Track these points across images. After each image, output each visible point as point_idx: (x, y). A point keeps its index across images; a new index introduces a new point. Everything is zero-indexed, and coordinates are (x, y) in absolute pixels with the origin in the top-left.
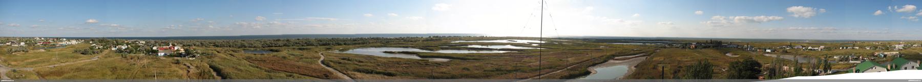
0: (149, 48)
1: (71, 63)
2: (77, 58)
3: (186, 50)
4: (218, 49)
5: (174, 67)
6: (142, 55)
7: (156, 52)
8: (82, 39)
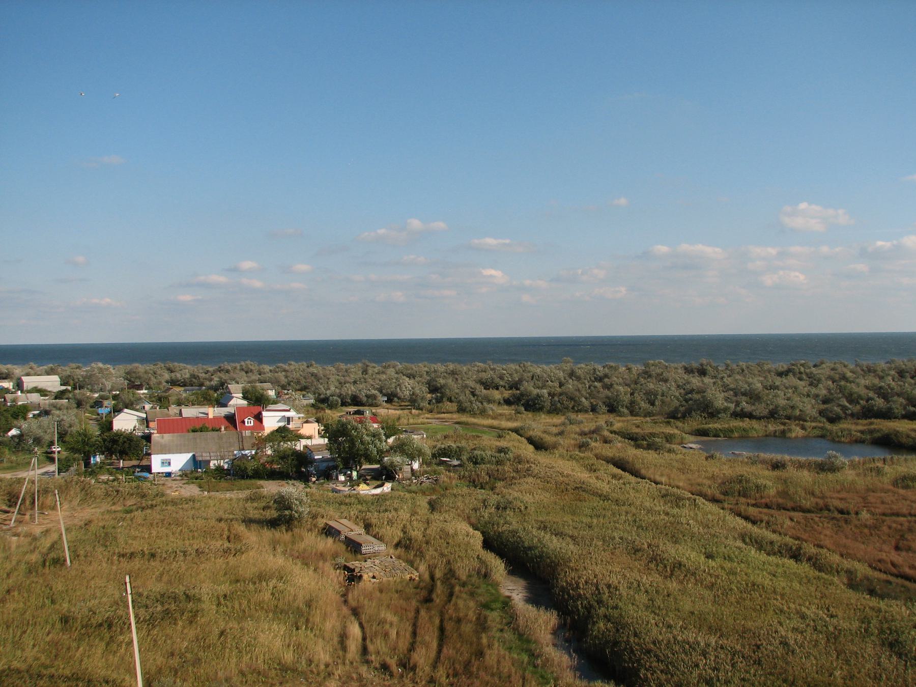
3: (334, 433)
5: (261, 551)
6: (35, 473)
7: (132, 448)
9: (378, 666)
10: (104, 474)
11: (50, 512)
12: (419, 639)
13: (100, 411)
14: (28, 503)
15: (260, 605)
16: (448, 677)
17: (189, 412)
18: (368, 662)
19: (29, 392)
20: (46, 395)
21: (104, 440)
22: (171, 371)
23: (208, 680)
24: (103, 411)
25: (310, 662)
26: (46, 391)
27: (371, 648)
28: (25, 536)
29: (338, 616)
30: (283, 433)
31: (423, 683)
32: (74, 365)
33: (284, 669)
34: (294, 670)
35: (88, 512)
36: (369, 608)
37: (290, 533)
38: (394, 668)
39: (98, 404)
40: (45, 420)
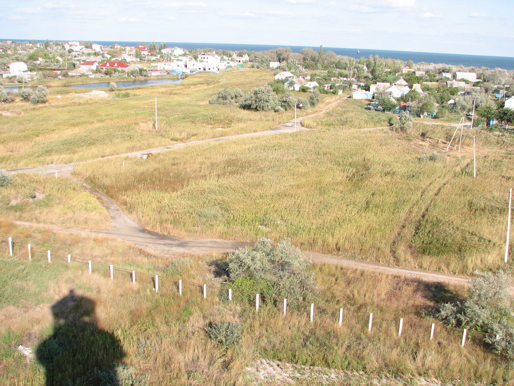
1: (205, 144)
2: (228, 122)
6: (460, 125)
8: (241, 50)
10: (497, 131)
11: (466, 147)
13: (497, 95)
14: (457, 141)
19: (460, 81)
20: (468, 84)
21: (500, 112)
24: (499, 96)
26: (468, 81)
28: (454, 157)
32: (484, 68)
35: (486, 151)
39: (497, 91)
40: (467, 97)
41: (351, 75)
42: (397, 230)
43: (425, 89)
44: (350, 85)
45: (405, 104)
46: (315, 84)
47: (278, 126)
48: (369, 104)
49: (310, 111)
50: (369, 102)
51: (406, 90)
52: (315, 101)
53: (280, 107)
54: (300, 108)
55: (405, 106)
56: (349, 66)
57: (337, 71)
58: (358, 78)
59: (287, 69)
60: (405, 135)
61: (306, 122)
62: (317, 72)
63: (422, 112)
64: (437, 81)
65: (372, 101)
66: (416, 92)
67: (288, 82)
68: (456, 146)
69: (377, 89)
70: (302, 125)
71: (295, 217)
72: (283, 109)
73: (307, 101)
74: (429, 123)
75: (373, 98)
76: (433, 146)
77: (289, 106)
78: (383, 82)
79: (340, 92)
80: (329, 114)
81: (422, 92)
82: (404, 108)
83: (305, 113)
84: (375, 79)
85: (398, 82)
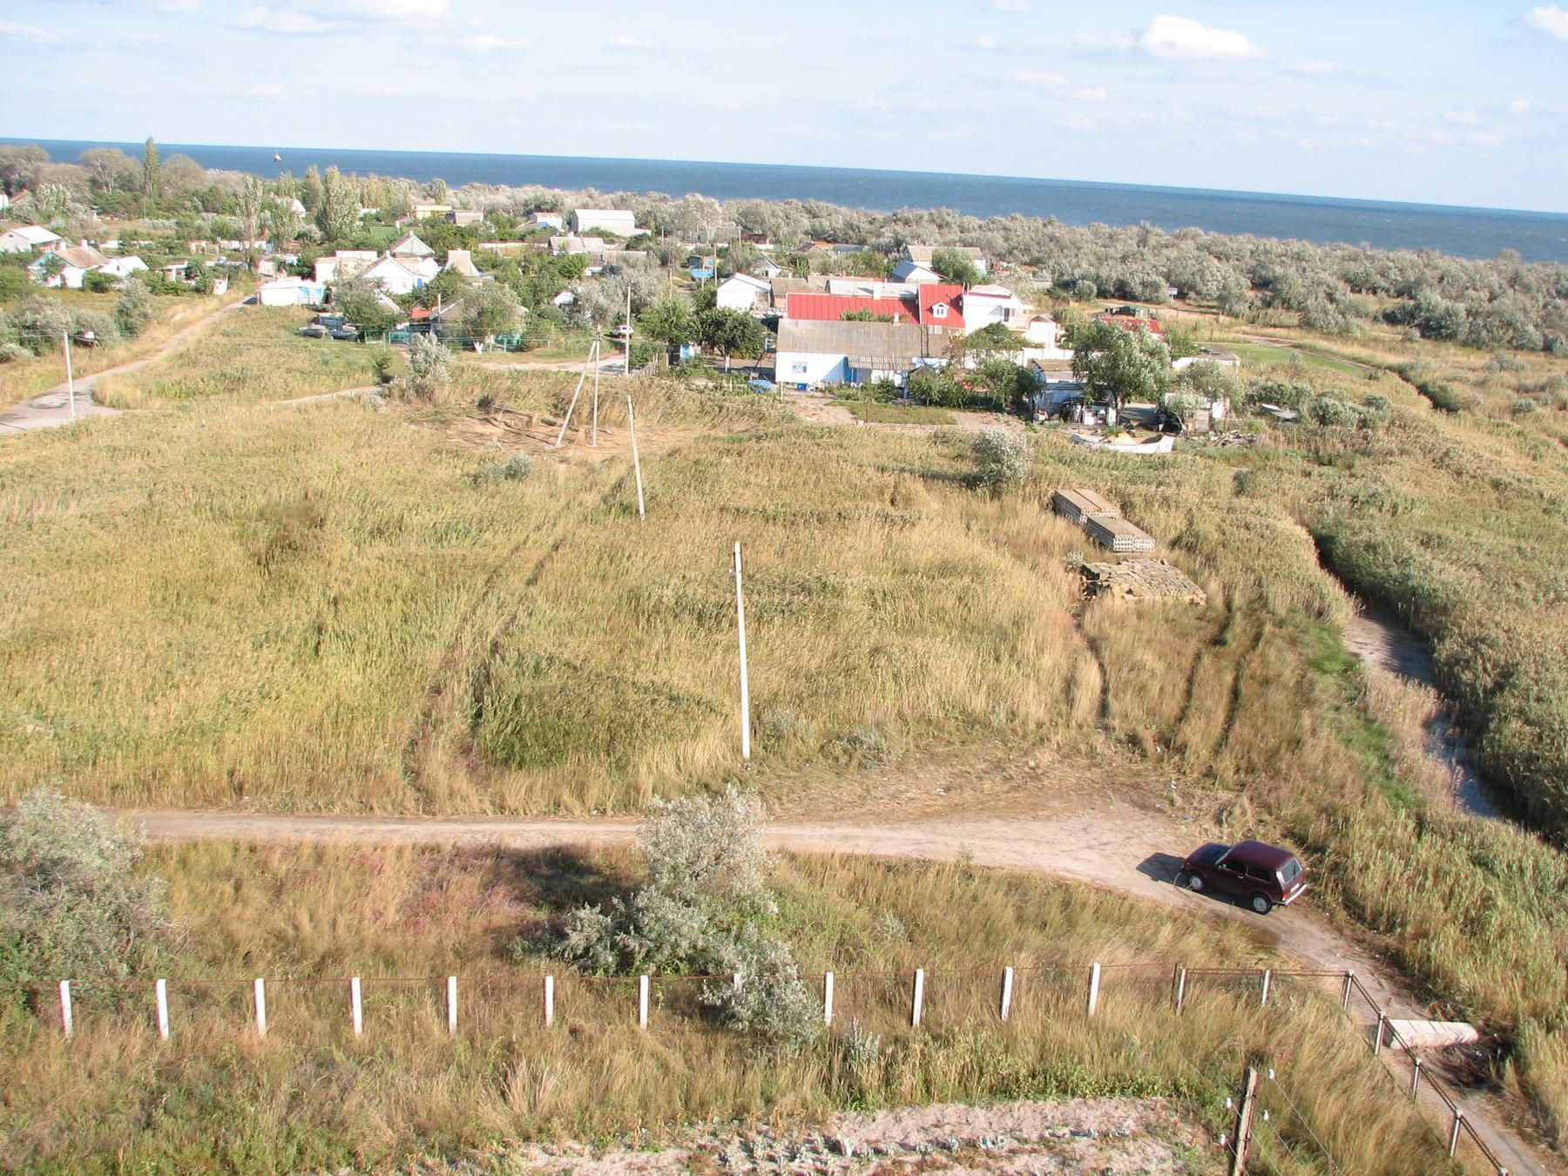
0: (668, 291)
3: (1083, 342)
4: (1442, 363)
5: (940, 528)
9: (1123, 737)
12: (1194, 703)
13: (696, 273)
14: (585, 414)
15: (939, 614)
16: (1237, 771)
17: (844, 286)
18: (1106, 728)
19: (587, 234)
20: (612, 242)
22: (814, 215)
23: (848, 722)
24: (702, 274)
25: (1013, 715)
26: (611, 234)
27: (1114, 706)
29: (1065, 647)
30: (995, 335)
31: (1195, 775)
32: (656, 195)
33: (971, 720)
34: (987, 725)
35: (673, 437)
36: (1121, 639)
37: (996, 503)
38: (1149, 744)
39: (694, 261)
40: (611, 281)
41: (255, 230)
42: (418, 704)
43: (485, 263)
44: (252, 263)
45: (425, 314)
46: (134, 263)
47: (15, 408)
48: (316, 321)
49: (120, 352)
50: (315, 315)
51: (430, 270)
52: (135, 320)
53: (14, 346)
54: (86, 344)
55: (426, 319)
56: (242, 202)
57: (208, 220)
58: (276, 239)
59: (34, 216)
60: (429, 408)
61: (110, 391)
62: (142, 224)
63: (480, 335)
64: (522, 239)
65: (324, 310)
66: (460, 275)
67: (42, 260)
68: (582, 430)
69: (338, 271)
70: (97, 399)
71: (85, 704)
72: (27, 352)
73: (110, 320)
74: (503, 367)
75: (327, 299)
76: (517, 435)
77: (48, 340)
78: (357, 247)
79: (221, 287)
80: (185, 359)
81: (476, 273)
82: (424, 326)
83: (105, 362)
84: (332, 241)
85: (401, 248)
